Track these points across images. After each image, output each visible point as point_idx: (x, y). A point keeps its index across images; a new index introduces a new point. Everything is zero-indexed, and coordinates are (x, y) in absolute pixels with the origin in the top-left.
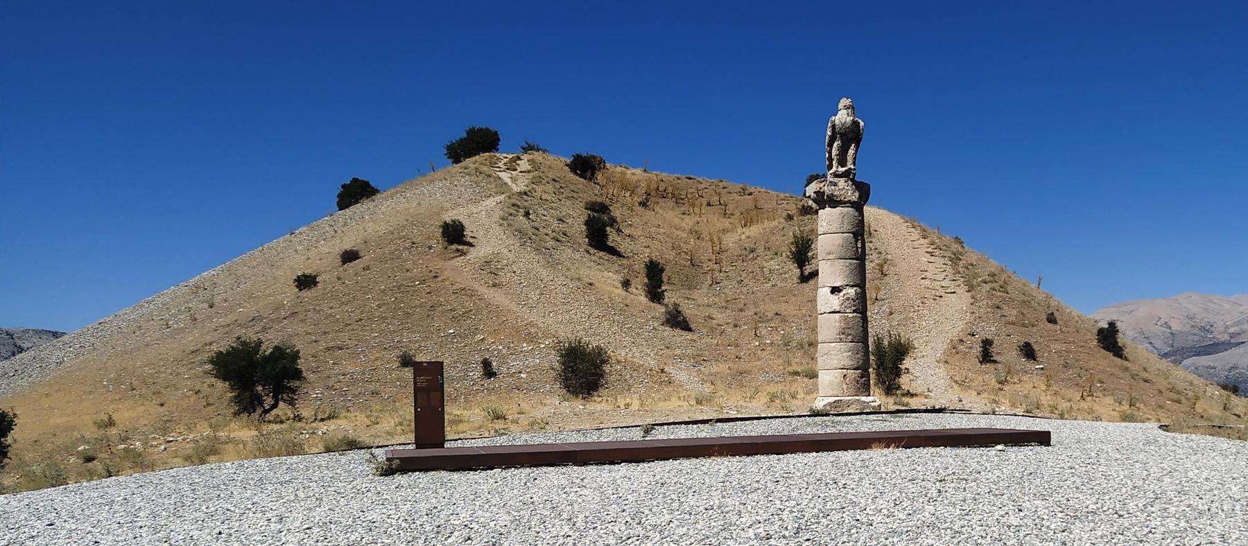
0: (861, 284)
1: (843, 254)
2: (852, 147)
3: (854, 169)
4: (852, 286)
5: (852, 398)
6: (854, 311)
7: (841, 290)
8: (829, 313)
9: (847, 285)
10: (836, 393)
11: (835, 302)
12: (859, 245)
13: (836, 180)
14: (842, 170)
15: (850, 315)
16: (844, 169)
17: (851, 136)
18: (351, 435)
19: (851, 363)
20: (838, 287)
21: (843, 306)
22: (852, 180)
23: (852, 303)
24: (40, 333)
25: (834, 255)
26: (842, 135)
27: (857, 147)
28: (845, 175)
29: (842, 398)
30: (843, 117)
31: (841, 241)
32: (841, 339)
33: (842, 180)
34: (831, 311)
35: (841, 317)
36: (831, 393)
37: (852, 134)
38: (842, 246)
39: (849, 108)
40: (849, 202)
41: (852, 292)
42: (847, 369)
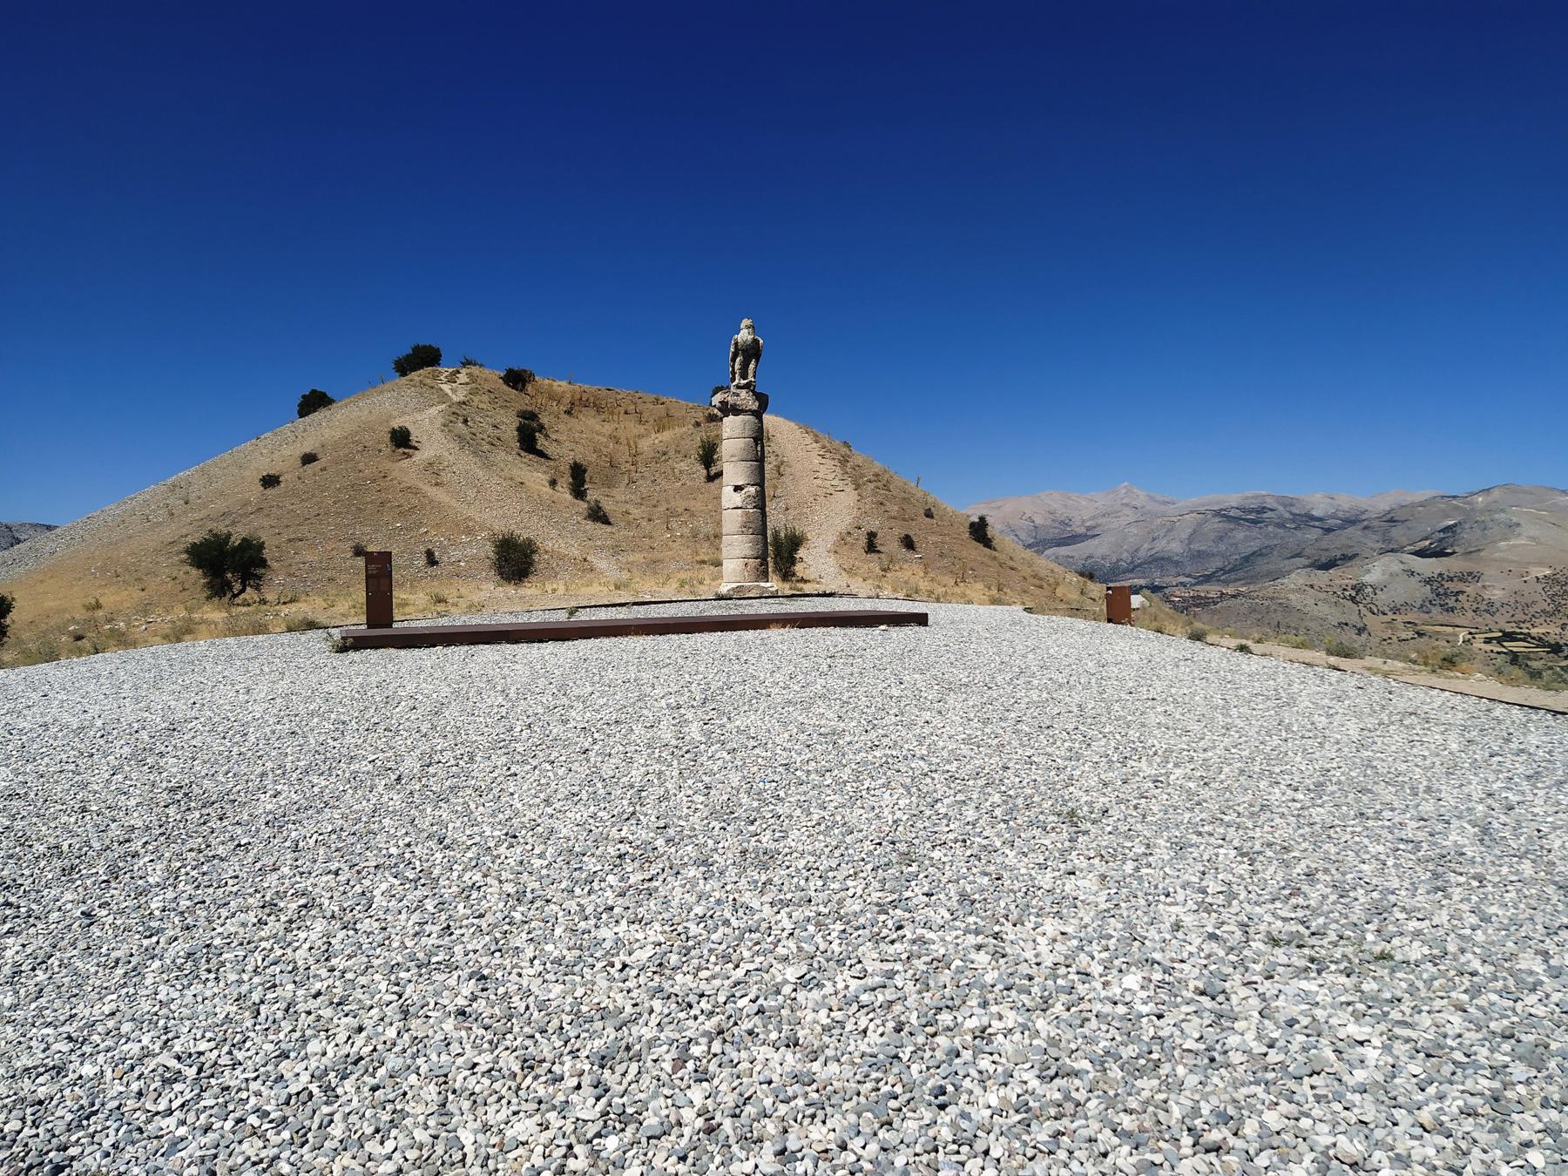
0: (760, 483)
1: (745, 457)
4: (753, 485)
6: (754, 507)
10: (738, 579)
11: (738, 499)
12: (759, 449)
13: (738, 391)
16: (745, 382)
17: (751, 352)
18: (310, 616)
19: (751, 553)
24: (35, 526)
27: (757, 362)
28: (747, 386)
30: (744, 336)
31: (743, 445)
33: (744, 391)
36: (734, 579)
40: (750, 410)
41: (752, 490)
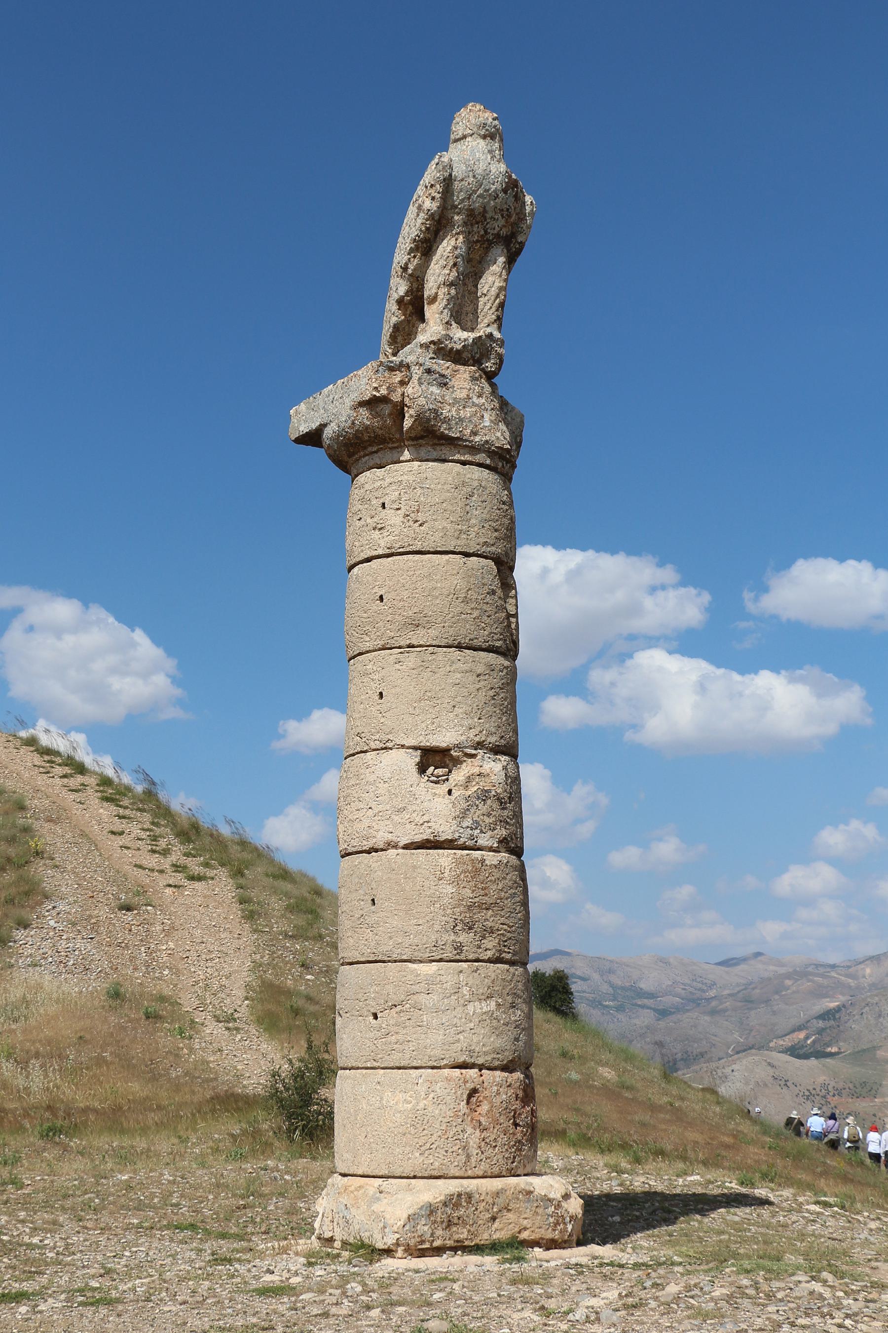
1: (466, 631)
3: (502, 343)
7: (457, 762)
8: (406, 847)
9: (479, 745)
13: (443, 366)
14: (461, 336)
15: (492, 858)
16: (471, 336)
19: (499, 1043)
21: (468, 822)
25: (433, 632)
26: (475, 218)
29: (471, 1185)
31: (458, 582)
32: (459, 948)
34: (418, 838)
35: (458, 862)
36: (416, 1162)
37: (502, 222)
38: (466, 601)
39: (492, 137)
40: (485, 448)
42: (481, 1067)
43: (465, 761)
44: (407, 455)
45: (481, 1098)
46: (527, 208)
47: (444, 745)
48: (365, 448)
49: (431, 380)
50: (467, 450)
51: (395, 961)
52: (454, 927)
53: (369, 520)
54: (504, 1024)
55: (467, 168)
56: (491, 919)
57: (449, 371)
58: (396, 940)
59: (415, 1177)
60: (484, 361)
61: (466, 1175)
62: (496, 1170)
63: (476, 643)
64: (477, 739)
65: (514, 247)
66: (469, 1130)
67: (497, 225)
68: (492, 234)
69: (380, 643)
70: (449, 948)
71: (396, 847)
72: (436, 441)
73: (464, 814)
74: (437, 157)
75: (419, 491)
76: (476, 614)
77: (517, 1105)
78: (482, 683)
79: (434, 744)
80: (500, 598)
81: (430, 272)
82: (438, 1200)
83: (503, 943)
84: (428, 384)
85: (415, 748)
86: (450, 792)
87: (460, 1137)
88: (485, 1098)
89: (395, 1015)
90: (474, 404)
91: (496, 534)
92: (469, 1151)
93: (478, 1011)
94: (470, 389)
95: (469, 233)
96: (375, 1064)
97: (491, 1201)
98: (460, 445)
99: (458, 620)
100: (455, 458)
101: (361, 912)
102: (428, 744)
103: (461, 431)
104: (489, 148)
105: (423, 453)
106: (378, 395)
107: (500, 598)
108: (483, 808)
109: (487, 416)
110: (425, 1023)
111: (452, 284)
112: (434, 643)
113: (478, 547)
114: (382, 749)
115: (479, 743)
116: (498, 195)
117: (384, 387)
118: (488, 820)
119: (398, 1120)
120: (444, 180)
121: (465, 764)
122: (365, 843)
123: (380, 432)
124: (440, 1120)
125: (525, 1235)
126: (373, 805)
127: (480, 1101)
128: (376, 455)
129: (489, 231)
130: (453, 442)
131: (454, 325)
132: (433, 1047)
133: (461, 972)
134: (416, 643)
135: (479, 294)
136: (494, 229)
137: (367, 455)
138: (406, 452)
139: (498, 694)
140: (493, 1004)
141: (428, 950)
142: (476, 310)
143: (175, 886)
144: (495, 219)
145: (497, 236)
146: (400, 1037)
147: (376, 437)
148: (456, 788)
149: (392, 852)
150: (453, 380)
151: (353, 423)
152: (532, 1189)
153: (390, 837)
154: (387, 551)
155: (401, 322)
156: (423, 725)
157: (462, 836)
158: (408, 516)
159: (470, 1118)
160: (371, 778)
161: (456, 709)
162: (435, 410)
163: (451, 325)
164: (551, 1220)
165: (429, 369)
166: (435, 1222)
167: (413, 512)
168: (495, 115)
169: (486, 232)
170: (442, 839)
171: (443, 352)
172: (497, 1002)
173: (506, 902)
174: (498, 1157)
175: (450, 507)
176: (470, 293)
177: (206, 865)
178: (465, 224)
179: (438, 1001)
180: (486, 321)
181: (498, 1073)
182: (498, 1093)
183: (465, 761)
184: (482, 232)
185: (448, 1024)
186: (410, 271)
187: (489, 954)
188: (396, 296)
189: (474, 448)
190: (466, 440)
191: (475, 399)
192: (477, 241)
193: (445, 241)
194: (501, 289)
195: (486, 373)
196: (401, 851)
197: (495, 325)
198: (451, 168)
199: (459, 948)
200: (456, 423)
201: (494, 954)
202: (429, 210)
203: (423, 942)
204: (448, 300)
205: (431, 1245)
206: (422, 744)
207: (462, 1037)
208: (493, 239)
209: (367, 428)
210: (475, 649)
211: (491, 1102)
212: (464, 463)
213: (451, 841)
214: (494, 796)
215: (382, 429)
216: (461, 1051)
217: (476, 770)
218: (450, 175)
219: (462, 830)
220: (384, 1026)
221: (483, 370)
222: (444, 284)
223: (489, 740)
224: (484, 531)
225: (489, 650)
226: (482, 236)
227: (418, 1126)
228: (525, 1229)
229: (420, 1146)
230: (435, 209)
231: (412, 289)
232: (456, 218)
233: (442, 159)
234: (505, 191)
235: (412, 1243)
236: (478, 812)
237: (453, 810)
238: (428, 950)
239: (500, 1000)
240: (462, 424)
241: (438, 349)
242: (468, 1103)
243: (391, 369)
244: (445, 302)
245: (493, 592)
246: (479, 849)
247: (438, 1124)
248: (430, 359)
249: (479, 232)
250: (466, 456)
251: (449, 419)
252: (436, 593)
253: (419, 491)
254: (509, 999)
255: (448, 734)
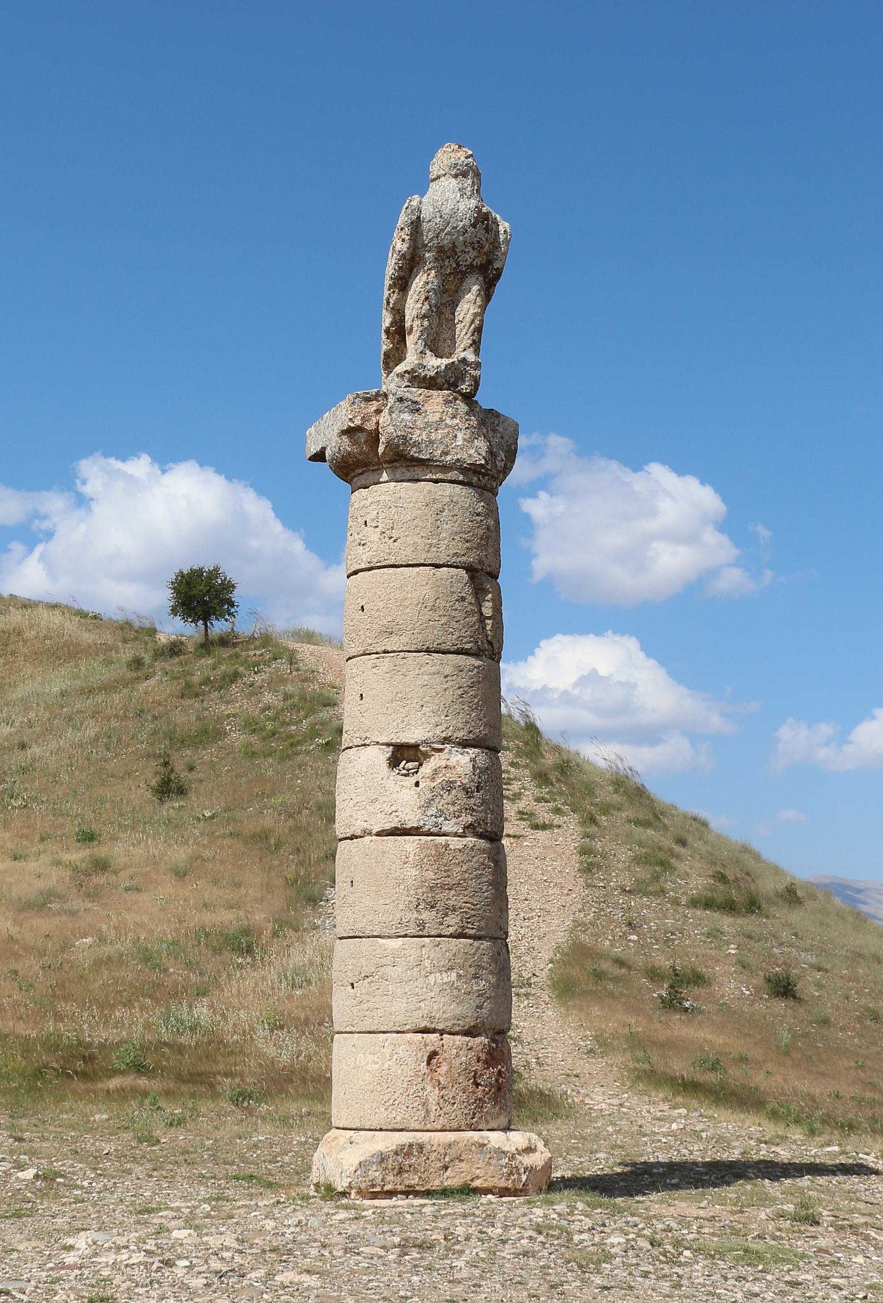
1: (433, 638)
2: (470, 296)
3: (478, 365)
4: (464, 744)
5: (451, 1136)
6: (470, 829)
7: (427, 756)
8: (378, 834)
9: (446, 740)
10: (398, 1117)
12: (487, 611)
13: (416, 393)
14: (434, 363)
15: (456, 843)
16: (445, 361)
19: (459, 1010)
20: (415, 747)
21: (432, 811)
22: (468, 398)
23: (463, 800)
25: (404, 639)
26: (444, 253)
27: (487, 294)
31: (427, 592)
32: (422, 925)
33: (438, 397)
34: (388, 826)
35: (422, 847)
36: (381, 1117)
37: (475, 253)
38: (434, 609)
39: (464, 175)
40: (457, 466)
42: (442, 1032)
43: (433, 755)
44: (385, 477)
45: (441, 1060)
46: (501, 236)
47: (412, 741)
48: (354, 470)
49: (403, 408)
50: (439, 469)
51: (369, 937)
52: (417, 906)
53: (356, 537)
54: (464, 993)
55: (434, 209)
56: (453, 898)
57: (421, 398)
58: (368, 918)
59: (381, 1130)
60: (459, 383)
61: (425, 1129)
62: (455, 1125)
63: (444, 647)
64: (444, 735)
65: (491, 274)
66: (429, 1088)
67: (469, 257)
68: (465, 266)
69: (361, 649)
70: (412, 925)
71: (370, 834)
72: (409, 463)
73: (429, 803)
74: (408, 201)
75: (393, 510)
76: (444, 620)
77: (479, 1067)
78: (450, 683)
79: (403, 740)
80: (470, 603)
81: (407, 305)
82: (390, 1149)
83: (467, 919)
84: (400, 412)
85: (388, 745)
86: (417, 784)
87: (420, 1094)
88: (444, 1059)
89: (367, 985)
90: (447, 426)
91: (468, 544)
92: (428, 1107)
93: (439, 981)
94: (444, 412)
95: (441, 267)
96: (353, 1029)
97: (443, 1151)
98: (431, 465)
99: (427, 627)
100: (427, 477)
101: (344, 893)
102: (399, 741)
103: (431, 453)
104: (460, 186)
105: (398, 476)
106: (352, 425)
107: (470, 603)
108: (448, 798)
109: (460, 436)
110: (391, 992)
111: (424, 317)
112: (405, 648)
113: (448, 558)
114: (362, 745)
115: (445, 739)
116: (466, 231)
117: (358, 418)
118: (452, 808)
119: (367, 1079)
120: (412, 223)
121: (433, 758)
122: (348, 830)
123: (360, 458)
124: (402, 1079)
125: (477, 1183)
126: (353, 796)
127: (440, 1063)
128: (362, 476)
129: (461, 263)
130: (424, 463)
131: (428, 353)
132: (397, 1013)
133: (424, 946)
134: (390, 649)
135: (456, 321)
136: (466, 261)
137: (356, 476)
138: (385, 474)
139: (467, 692)
140: (453, 976)
141: (394, 927)
142: (454, 336)
143: (514, 837)
144: (465, 252)
145: (471, 266)
146: (370, 1005)
147: (358, 461)
148: (423, 780)
149: (368, 839)
150: (426, 405)
151: (339, 449)
152: (486, 1142)
153: (365, 825)
154: (368, 566)
155: (390, 350)
156: (395, 724)
157: (427, 823)
158: (384, 533)
159: (429, 1077)
160: (353, 772)
161: (424, 708)
162: (403, 436)
163: (425, 354)
164: (505, 1170)
165: (401, 398)
166: (386, 1168)
167: (388, 529)
168: (470, 152)
169: (458, 265)
170: (408, 826)
171: (418, 380)
172: (458, 973)
173: (470, 882)
174: (457, 1113)
175: (420, 524)
176: (448, 320)
177: (557, 811)
178: (436, 260)
179: (402, 973)
180: (462, 346)
181: (458, 1037)
182: (458, 1055)
183: (433, 755)
184: (454, 265)
185: (410, 993)
186: (391, 306)
187: (451, 930)
188: (384, 328)
189: (446, 467)
190: (437, 461)
191: (449, 421)
192: (450, 274)
193: (418, 277)
194: (475, 315)
195: (462, 394)
196: (374, 837)
197: (471, 349)
198: (420, 210)
199: (422, 925)
200: (427, 446)
201: (457, 930)
202: (400, 251)
203: (390, 920)
204: (421, 331)
205: (382, 1189)
206: (393, 741)
207: (423, 1005)
208: (466, 270)
209: (349, 454)
210: (444, 653)
211: (450, 1064)
212: (436, 481)
213: (417, 828)
214: (460, 786)
215: (360, 455)
216: (423, 1017)
217: (443, 763)
218: (419, 218)
219: (426, 819)
220: (358, 994)
221: (459, 392)
222: (417, 317)
223: (455, 735)
224: (454, 543)
225: (458, 652)
226: (455, 268)
227: (383, 1084)
228: (478, 1177)
229: (385, 1102)
230: (405, 249)
231: (396, 321)
232: (427, 255)
233: (412, 203)
234: (474, 226)
235: (363, 1186)
236: (443, 802)
237: (418, 800)
238: (394, 927)
239: (461, 972)
240: (433, 446)
241: (412, 377)
242: (428, 1064)
243: (367, 400)
244: (418, 334)
245: (463, 599)
246: (444, 835)
247: (400, 1083)
248: (406, 387)
249: (451, 265)
250: (438, 475)
251: (419, 443)
252: (407, 603)
253: (393, 510)
254: (472, 970)
255: (416, 731)
